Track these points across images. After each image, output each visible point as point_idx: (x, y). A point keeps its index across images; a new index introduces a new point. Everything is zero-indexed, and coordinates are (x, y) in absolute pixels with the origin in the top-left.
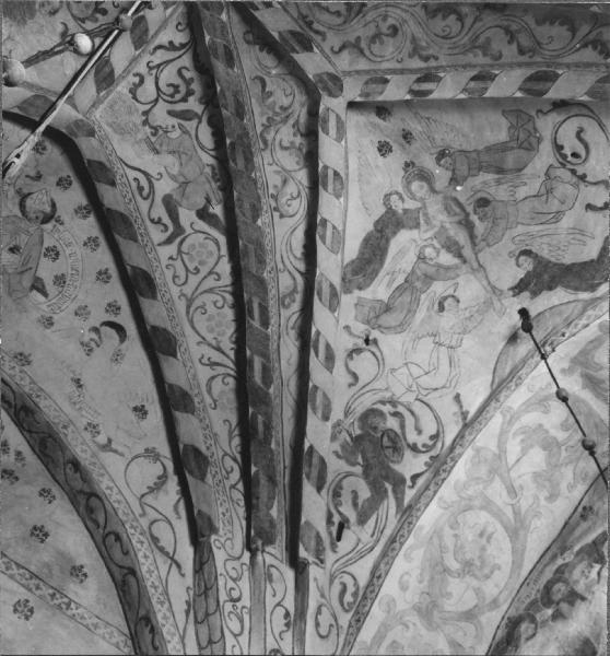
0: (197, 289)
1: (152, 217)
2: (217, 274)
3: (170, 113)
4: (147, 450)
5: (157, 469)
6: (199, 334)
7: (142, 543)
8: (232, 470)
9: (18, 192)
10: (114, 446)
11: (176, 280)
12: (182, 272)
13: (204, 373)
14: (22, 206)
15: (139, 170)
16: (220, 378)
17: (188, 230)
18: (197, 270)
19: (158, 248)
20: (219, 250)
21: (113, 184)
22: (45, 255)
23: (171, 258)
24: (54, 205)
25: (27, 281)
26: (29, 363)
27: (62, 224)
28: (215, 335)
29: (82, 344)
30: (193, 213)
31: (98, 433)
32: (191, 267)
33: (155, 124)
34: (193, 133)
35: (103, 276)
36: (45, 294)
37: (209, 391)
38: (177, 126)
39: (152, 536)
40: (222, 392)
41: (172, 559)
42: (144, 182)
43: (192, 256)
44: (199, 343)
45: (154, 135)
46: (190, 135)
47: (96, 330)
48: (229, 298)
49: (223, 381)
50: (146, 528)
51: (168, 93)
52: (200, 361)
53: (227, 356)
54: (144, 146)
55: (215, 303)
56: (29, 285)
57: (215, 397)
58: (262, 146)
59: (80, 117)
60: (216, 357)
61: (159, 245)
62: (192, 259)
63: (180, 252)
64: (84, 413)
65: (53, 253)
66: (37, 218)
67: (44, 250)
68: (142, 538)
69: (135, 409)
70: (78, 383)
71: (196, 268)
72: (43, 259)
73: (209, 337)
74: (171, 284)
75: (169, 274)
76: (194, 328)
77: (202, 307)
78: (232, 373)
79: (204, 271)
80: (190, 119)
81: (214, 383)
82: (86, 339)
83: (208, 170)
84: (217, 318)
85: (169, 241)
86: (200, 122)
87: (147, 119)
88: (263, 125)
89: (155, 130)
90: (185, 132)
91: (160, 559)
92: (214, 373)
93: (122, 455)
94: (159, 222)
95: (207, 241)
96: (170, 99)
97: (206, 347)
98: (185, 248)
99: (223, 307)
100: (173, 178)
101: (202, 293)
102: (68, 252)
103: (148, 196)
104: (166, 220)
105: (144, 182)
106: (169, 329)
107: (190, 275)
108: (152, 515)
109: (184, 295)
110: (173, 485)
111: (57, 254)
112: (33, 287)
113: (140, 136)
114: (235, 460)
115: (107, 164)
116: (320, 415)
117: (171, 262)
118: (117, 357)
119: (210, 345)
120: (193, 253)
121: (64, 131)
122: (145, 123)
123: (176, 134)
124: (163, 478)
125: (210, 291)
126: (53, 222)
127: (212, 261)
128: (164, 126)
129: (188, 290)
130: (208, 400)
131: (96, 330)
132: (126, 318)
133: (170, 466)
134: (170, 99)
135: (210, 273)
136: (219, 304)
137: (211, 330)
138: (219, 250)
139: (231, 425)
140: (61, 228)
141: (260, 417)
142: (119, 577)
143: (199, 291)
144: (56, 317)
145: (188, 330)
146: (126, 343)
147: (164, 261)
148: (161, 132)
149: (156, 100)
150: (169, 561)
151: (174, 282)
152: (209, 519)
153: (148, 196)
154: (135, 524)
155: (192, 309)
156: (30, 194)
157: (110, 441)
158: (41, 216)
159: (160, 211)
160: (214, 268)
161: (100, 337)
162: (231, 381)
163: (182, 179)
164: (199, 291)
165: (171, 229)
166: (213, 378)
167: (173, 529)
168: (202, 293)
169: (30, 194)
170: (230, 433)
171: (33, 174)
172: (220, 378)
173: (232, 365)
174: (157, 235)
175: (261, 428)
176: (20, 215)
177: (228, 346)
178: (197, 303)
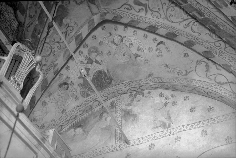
0: (164, 13)
1: (137, 11)
4: (197, 63)
5: (204, 64)
6: (177, 22)
7: (216, 88)
8: (220, 44)
9: (111, 42)
10: (188, 71)
13: (188, 30)
14: (115, 44)
15: (123, 5)
16: (193, 26)
19: (146, 16)
21: (122, 17)
22: (130, 48)
24: (120, 36)
25: (133, 58)
26: (153, 74)
27: (125, 37)
28: (180, 18)
29: (158, 56)
31: (182, 72)
32: (157, 10)
35: (145, 36)
36: (140, 56)
37: (194, 32)
39: (218, 83)
40: (198, 28)
41: (229, 82)
42: (127, 6)
44: (179, 25)
47: (157, 49)
48: (173, 5)
49: (195, 26)
50: (214, 83)
52: (184, 28)
53: (189, 19)
55: (172, 11)
56: (134, 58)
57: (198, 32)
59: (100, 14)
60: (187, 22)
63: (151, 10)
64: (174, 71)
65: (131, 45)
67: (129, 47)
68: (215, 87)
69: (184, 56)
70: (166, 66)
71: (158, 8)
72: (131, 49)
73: (180, 20)
74: (159, 20)
76: (174, 22)
78: (194, 21)
81: (193, 29)
82: (157, 54)
85: (146, 11)
91: (225, 86)
92: (191, 26)
93: (192, 71)
94: (140, 10)
97: (182, 23)
98: (151, 8)
99: (174, 9)
101: (166, 13)
102: (133, 41)
103: (131, 7)
104: (140, 7)
105: (127, 6)
106: (169, 31)
107: (159, 12)
108: (212, 77)
109: (164, 18)
110: (211, 64)
111: (132, 44)
112: (136, 57)
114: (219, 41)
115: (116, 15)
116: (224, 7)
117: (152, 15)
118: (168, 50)
119: (182, 22)
120: (154, 6)
121: (101, 21)
124: (207, 65)
125: (167, 9)
126: (124, 39)
129: (163, 16)
130: (196, 35)
131: (157, 49)
132: (160, 39)
133: (205, 60)
135: (162, 5)
136: (173, 10)
139: (208, 34)
140: (126, 38)
141: (211, 25)
142: (221, 100)
143: (165, 13)
144: (146, 58)
145: (173, 25)
146: (166, 44)
150: (228, 84)
152: (226, 64)
154: (210, 85)
156: (113, 40)
157: (186, 71)
158: (120, 41)
161: (160, 50)
162: (196, 23)
164: (165, 13)
165: (144, 8)
166: (192, 28)
167: (221, 75)
168: (166, 13)
169: (113, 40)
170: (210, 35)
171: (109, 35)
172: (193, 26)
173: (192, 20)
174: (142, 14)
175: (214, 28)
176: (117, 46)
177: (186, 16)
178: (168, 16)
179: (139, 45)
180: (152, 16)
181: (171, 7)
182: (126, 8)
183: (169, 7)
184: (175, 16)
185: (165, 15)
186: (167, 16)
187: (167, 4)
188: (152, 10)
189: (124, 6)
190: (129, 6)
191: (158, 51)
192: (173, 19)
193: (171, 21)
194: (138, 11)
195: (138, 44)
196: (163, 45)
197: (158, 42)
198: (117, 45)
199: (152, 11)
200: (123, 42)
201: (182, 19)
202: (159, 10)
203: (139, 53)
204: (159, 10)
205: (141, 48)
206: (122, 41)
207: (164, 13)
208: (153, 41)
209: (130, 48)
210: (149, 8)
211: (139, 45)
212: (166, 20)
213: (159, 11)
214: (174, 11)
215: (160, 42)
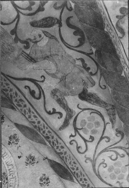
0: (95, 151)
1: (48, 110)
2: (107, 137)
3: (33, 24)
11: (80, 150)
12: (81, 142)
15: (25, 79)
17: (77, 110)
18: (92, 138)
20: (103, 120)
23: (71, 136)
28: (117, 180)
30: (77, 97)
32: (87, 137)
33: (24, 39)
34: (58, 36)
38: (43, 35)
42: (33, 87)
43: (85, 129)
45: (27, 47)
46: (56, 39)
51: (25, 7)
54: (23, 59)
58: (120, 35)
61: (60, 129)
62: (86, 131)
63: (76, 130)
75: (73, 148)
77: (103, 163)
79: (97, 137)
80: (50, 26)
83: (79, 63)
84: (115, 168)
85: (66, 124)
86: (60, 25)
87: (16, 36)
88: (117, 17)
89: (27, 43)
90: (52, 37)
94: (54, 112)
95: (92, 114)
96: (27, 12)
98: (78, 126)
99: (117, 158)
100: (54, 76)
101: (100, 153)
103: (40, 95)
104: (59, 109)
105: (33, 87)
107: (88, 143)
113: (16, 53)
117: (72, 138)
120: (86, 127)
122: (17, 40)
123: (44, 42)
125: (105, 150)
127: (100, 129)
128: (32, 38)
134: (27, 12)
135: (102, 138)
136: (114, 157)
137: (113, 177)
138: (103, 120)
147: (67, 140)
148: (31, 44)
149: (18, 17)
151: (79, 152)
153: (40, 95)
155: (97, 168)
159: (52, 104)
160: (103, 134)
163: (60, 75)
164: (99, 151)
168: (100, 153)
178: (100, 160)
179: (8, 172)
180: (69, 140)
181: (115, 152)
182: (30, 89)
183: (111, 149)
184: (110, 170)
185: (94, 155)
186: (96, 160)
187: (111, 141)
188: (78, 130)
189: (27, 83)
190: (39, 89)
192: (103, 171)
194: (50, 111)
195: (7, 169)
199: (77, 131)
201: (118, 183)
202: (91, 140)
204: (91, 140)
205: (9, 179)
207: (95, 151)
208: (41, 180)
210: (75, 120)
211: (8, 172)
212: (89, 164)
214: (114, 160)
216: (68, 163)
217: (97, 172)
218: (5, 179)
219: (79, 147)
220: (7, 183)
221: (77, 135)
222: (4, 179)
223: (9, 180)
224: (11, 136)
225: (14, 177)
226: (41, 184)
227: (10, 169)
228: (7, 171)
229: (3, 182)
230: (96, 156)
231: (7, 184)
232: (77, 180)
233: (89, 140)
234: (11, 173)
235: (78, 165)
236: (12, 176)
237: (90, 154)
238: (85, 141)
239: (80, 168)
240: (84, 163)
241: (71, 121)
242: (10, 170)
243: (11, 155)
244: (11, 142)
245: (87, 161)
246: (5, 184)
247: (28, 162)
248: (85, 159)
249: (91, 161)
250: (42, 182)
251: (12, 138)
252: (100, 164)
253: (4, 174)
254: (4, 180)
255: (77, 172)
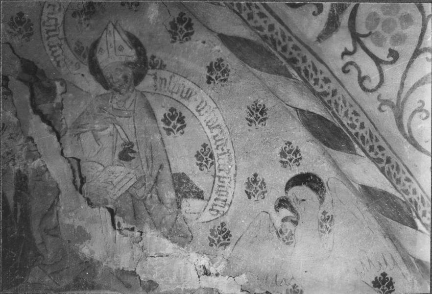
0: (402, 84)
9: (78, 51)
11: (366, 84)
12: (368, 67)
14: (95, 70)
18: (394, 55)
22: (169, 131)
23: (346, 53)
32: (382, 53)
43: (377, 34)
47: (283, 203)
62: (379, 43)
63: (356, 38)
66: (125, 77)
67: (162, 125)
71: (390, 50)
72: (169, 139)
75: (351, 81)
85: (332, 24)
98: (362, 29)
117: (348, 59)
131: (283, 203)
140: (164, 74)
143: (405, 91)
144: (227, 219)
146: (328, 196)
147: (337, 64)
151: (364, 89)
158: (129, 72)
161: (292, 210)
176: (103, 91)
179: (213, 142)
180: (341, 63)
185: (399, 94)
186: (404, 102)
188: (362, 39)
191: (285, 212)
193: (410, 130)
195: (210, 135)
196: (313, 194)
197: (297, 171)
198: (104, 82)
199: (359, 41)
200: (142, 86)
202: (391, 59)
203: (201, 180)
204: (391, 59)
205: (215, 155)
206: (139, 77)
207: (402, 84)
208: (283, 154)
209: (164, 132)
211: (213, 142)
212: (388, 112)
213: (387, 63)
215: (308, 175)
216: (341, 114)
217: (407, 131)
218: (208, 157)
219: (364, 78)
220: (212, 164)
221: (360, 51)
222: (205, 157)
223: (216, 159)
224: (211, 64)
225: (226, 151)
226: (282, 162)
227: (217, 135)
228: (211, 140)
229: (204, 163)
230: (403, 96)
231: (214, 166)
232: (364, 151)
233: (387, 59)
234: (218, 143)
235: (362, 118)
236: (223, 150)
237: (390, 91)
238: (378, 62)
239: (367, 124)
240: (377, 112)
241: (345, 19)
242: (217, 138)
243: (215, 106)
244: (213, 77)
245: (384, 108)
246: (208, 166)
247: (252, 118)
248: (379, 103)
249: (393, 107)
250: (284, 160)
251: (214, 67)
252: (414, 112)
253: (205, 148)
254: (206, 159)
255: (362, 132)
